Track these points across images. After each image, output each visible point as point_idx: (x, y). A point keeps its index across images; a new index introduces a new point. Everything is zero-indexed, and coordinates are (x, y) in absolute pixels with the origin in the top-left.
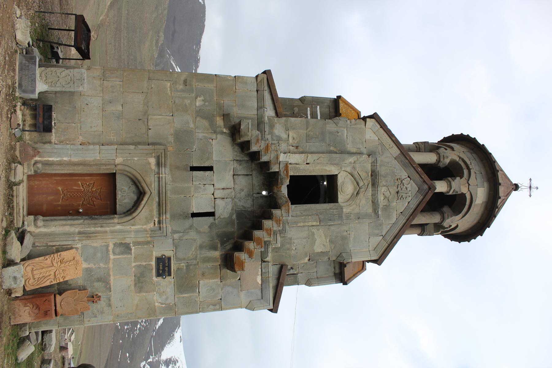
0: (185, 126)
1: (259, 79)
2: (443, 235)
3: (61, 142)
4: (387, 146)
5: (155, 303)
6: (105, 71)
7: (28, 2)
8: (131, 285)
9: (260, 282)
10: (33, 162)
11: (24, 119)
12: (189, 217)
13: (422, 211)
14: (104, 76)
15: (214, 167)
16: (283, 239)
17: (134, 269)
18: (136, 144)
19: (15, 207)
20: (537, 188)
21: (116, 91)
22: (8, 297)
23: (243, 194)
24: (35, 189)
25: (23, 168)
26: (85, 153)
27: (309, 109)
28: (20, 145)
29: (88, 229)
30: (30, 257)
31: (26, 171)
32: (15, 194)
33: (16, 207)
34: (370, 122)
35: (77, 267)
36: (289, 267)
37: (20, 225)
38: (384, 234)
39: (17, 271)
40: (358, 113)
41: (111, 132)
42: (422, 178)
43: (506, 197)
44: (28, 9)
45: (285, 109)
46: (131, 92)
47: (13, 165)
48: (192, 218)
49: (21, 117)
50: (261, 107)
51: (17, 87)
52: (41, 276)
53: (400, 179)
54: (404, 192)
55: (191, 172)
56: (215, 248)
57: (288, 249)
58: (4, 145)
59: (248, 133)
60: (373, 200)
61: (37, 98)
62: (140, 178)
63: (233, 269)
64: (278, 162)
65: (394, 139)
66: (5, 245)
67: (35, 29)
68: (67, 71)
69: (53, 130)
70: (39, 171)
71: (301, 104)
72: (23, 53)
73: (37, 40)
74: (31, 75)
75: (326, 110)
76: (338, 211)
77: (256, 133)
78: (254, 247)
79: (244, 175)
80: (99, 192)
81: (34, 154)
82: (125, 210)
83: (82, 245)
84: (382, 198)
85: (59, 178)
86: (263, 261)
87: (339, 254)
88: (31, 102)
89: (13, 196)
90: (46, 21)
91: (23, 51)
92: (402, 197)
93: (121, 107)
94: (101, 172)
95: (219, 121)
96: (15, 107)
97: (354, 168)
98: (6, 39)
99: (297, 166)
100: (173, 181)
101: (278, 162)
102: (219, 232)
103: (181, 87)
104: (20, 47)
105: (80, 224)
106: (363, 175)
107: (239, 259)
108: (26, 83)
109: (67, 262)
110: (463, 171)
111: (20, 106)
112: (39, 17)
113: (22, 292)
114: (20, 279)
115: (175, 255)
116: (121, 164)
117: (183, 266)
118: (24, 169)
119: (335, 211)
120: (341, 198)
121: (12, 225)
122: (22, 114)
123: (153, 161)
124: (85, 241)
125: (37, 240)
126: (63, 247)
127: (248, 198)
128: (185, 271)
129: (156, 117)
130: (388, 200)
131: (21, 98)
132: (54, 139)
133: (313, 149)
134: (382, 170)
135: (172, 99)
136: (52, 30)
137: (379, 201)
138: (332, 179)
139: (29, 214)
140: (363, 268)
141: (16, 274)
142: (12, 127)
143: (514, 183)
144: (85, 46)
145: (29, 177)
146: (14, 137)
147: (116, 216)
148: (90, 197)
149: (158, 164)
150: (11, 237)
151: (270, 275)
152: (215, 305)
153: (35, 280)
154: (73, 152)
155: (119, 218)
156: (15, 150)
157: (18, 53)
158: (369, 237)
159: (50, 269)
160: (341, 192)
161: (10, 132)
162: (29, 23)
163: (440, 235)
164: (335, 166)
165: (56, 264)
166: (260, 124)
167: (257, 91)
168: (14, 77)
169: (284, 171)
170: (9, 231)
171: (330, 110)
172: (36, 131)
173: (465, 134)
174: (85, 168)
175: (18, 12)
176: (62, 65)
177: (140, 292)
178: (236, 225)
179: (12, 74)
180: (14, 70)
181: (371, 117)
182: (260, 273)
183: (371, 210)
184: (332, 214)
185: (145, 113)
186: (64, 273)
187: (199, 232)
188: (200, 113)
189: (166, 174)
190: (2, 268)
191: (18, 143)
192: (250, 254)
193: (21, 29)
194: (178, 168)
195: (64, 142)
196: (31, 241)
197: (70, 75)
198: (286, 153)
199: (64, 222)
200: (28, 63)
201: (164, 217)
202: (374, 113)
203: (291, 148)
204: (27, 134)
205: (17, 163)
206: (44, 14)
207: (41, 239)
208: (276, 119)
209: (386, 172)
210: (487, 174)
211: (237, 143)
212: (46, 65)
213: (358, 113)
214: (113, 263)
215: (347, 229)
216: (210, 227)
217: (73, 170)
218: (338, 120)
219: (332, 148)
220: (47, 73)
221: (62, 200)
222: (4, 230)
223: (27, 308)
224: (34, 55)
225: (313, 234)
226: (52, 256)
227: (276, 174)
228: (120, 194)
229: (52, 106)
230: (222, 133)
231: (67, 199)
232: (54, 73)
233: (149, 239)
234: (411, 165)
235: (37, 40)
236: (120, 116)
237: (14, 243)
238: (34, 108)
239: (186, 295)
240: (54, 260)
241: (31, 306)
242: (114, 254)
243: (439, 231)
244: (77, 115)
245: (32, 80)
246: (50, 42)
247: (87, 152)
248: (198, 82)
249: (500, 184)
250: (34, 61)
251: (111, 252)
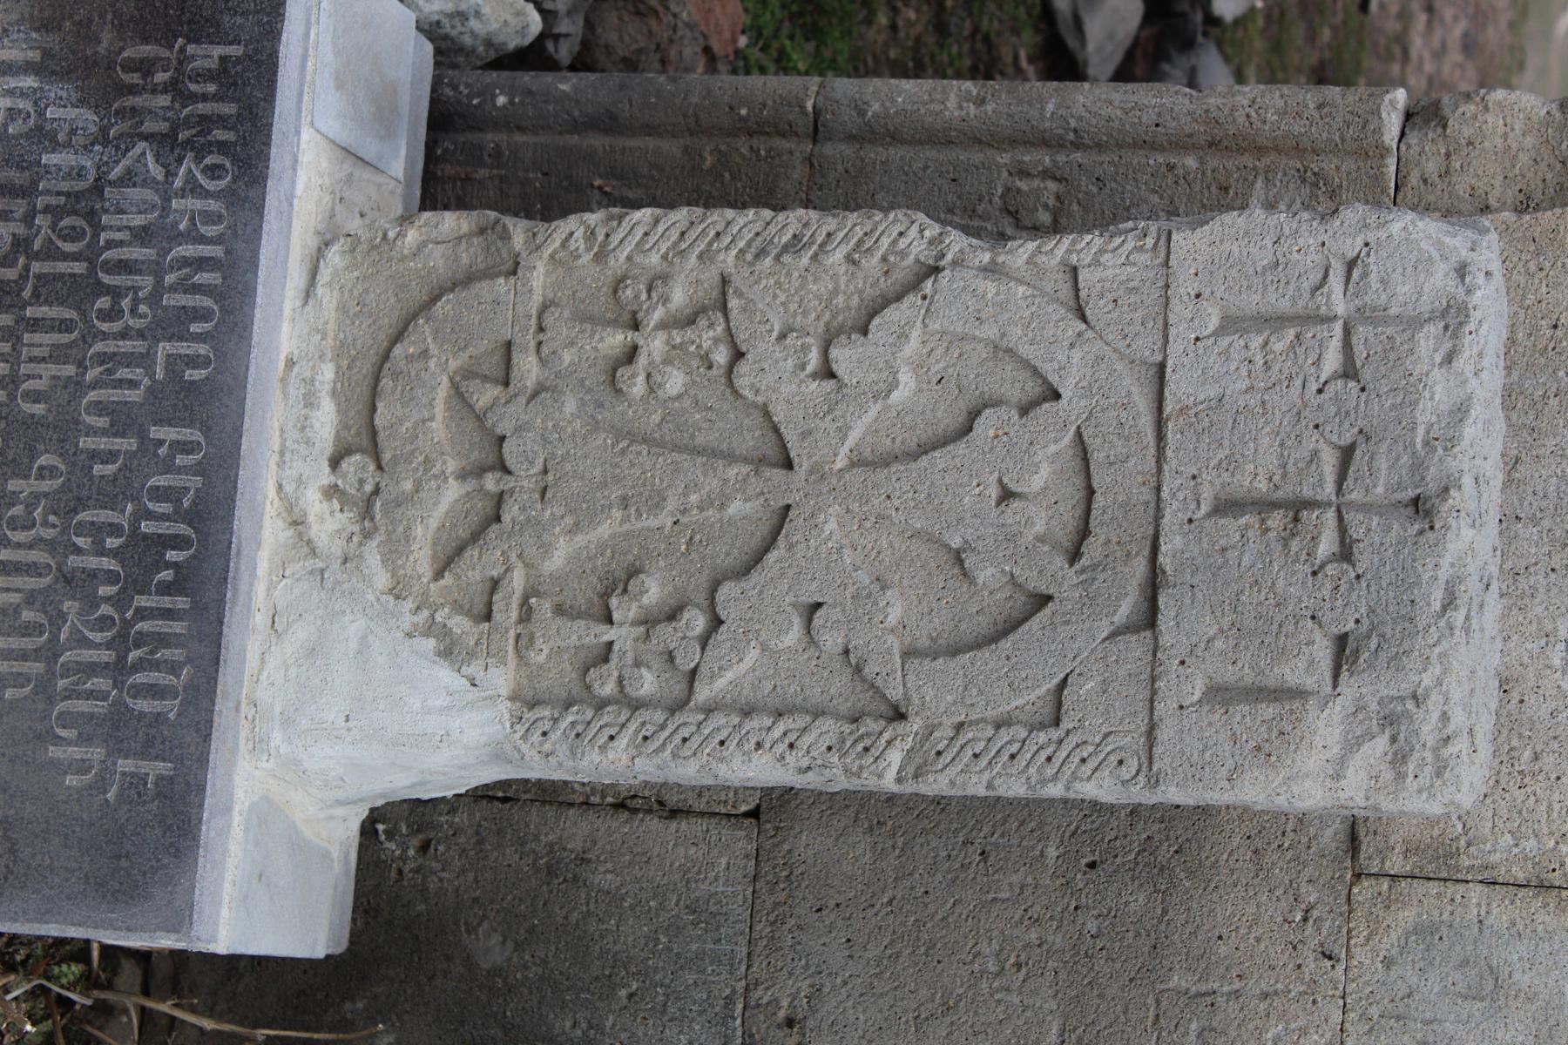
74: (121, 420)
197: (1072, 404)
200: (87, 118)
212: (609, 123)
220: (528, 368)
232: (676, 354)
250: (223, 73)
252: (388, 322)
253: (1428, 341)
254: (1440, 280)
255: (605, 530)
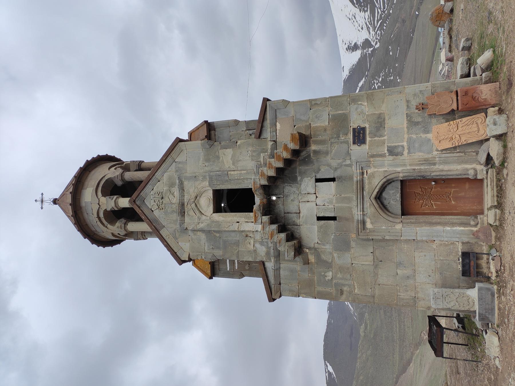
0: (341, 255)
1: (279, 294)
2: (122, 161)
3: (453, 244)
4: (171, 236)
5: (367, 105)
6: (414, 305)
7: (488, 371)
8: (388, 120)
9: (278, 123)
10: (479, 226)
11: (488, 264)
12: (337, 178)
13: (141, 182)
14: (415, 301)
15: (316, 220)
16: (258, 160)
17: (386, 133)
18: (384, 240)
19: (495, 187)
20: (36, 201)
21: (403, 287)
22: (502, 107)
23: (292, 198)
24: (476, 202)
25: (487, 221)
26: (430, 233)
27: (236, 268)
28: (491, 242)
29: (427, 167)
30: (481, 142)
31: (485, 218)
32: (495, 199)
33: (494, 186)
34: (185, 257)
35: (438, 134)
36: (253, 136)
37: (490, 171)
38: (174, 163)
39: (493, 131)
40: (195, 264)
41: (407, 250)
42: (141, 210)
43: (64, 193)
44: (488, 364)
45: (256, 268)
46: (389, 285)
47: (497, 223)
48: (335, 177)
49: (491, 266)
50: (277, 270)
51: (496, 293)
52: (470, 126)
53: (160, 209)
54: (157, 198)
55: (335, 216)
56: (315, 152)
57: (254, 151)
58: (507, 242)
59: (288, 248)
60: (183, 192)
61: (476, 283)
62: (380, 211)
63: (300, 135)
64: (262, 224)
65: (165, 243)
66: (505, 153)
67: (481, 346)
68: (449, 306)
69: (460, 254)
70: (473, 218)
71: (242, 272)
72: (491, 324)
73: (479, 336)
74: (483, 304)
75: (222, 266)
76: (213, 182)
77: (281, 249)
78: (282, 153)
79: (291, 213)
80: (416, 199)
81: (478, 233)
82: (393, 184)
83: (432, 154)
84: (175, 193)
85: (454, 211)
86: (275, 141)
87: (211, 147)
88: (482, 279)
89: (497, 196)
90: (471, 352)
91: (492, 326)
92: (159, 194)
93: (398, 272)
94: (415, 217)
95: (312, 258)
96: (497, 275)
97: (199, 219)
98: (508, 338)
99: (246, 221)
100: (350, 208)
101: (262, 224)
102: (312, 166)
103: (345, 289)
104: (494, 330)
105: (434, 171)
106: (191, 213)
107: (295, 143)
108: (487, 297)
109: (446, 139)
110: (103, 215)
111: (492, 276)
112: (477, 357)
113: (488, 112)
114: (490, 123)
115: (349, 146)
116: (397, 223)
117: (342, 137)
118: (487, 219)
119: (215, 183)
120: (210, 194)
121: (497, 170)
122: (490, 269)
123: (369, 225)
124: (430, 157)
125: (474, 157)
126: (450, 152)
127: (288, 193)
128: (341, 133)
129: (367, 263)
130: (170, 192)
131: (492, 284)
132: (459, 246)
133: (233, 234)
134: (175, 216)
135: (353, 278)
136: (464, 343)
137: (178, 191)
138: (217, 209)
139: (482, 180)
140: (191, 134)
141: (494, 127)
142: (499, 258)
143: (57, 205)
144: (433, 328)
145: (482, 213)
146: (497, 249)
147: (401, 179)
148: (424, 195)
149: (364, 223)
150: (499, 160)
151: (269, 130)
152: (316, 104)
153: (476, 123)
154: (441, 234)
155: (398, 177)
156: (496, 237)
157: (496, 324)
158: (186, 161)
159: (462, 133)
160: (210, 198)
161: (501, 253)
162: (486, 351)
163: (124, 161)
164: (215, 220)
165: (456, 137)
166: (278, 255)
167: (280, 284)
168: (500, 303)
169: (258, 216)
170: (500, 165)
171: (218, 266)
172: (477, 253)
173: (101, 248)
174: (430, 220)
175: (497, 362)
176: (454, 312)
177: (380, 114)
178: (298, 172)
179: (501, 306)
180: (499, 309)
181: (185, 261)
182: (278, 131)
183: (185, 184)
184: (218, 180)
185: (376, 266)
186: (449, 129)
187: (329, 165)
188: (328, 265)
189: (357, 214)
190: (507, 133)
191: (493, 243)
192: (286, 147)
193: (494, 346)
194: (347, 219)
195: (450, 243)
196: (479, 157)
197: (446, 302)
198: (256, 231)
199: (449, 173)
201: (358, 178)
202: (181, 265)
203: (251, 235)
204: (485, 251)
205: (494, 226)
206: (473, 360)
207: (471, 159)
208: (264, 260)
209: (172, 215)
210: (82, 213)
211: (297, 240)
213: (194, 264)
214: (404, 138)
215: (205, 168)
216: (319, 170)
217: (441, 218)
218: (212, 259)
219: (218, 235)
220: (467, 305)
221: (451, 192)
222: (506, 167)
223: (484, 98)
224: (481, 322)
225: (233, 164)
226: (460, 144)
227: (264, 214)
228: (397, 197)
229: (462, 276)
230: (309, 248)
231: (446, 193)
233: (372, 159)
234: (150, 221)
235: (479, 336)
236: (399, 264)
237: (496, 155)
238: (479, 274)
239: (340, 112)
240: (458, 140)
241: (480, 99)
242: (403, 147)
243: (125, 164)
244: (439, 266)
245: (482, 299)
246: (466, 333)
247: (429, 234)
248: (331, 293)
249: (70, 205)
251: (406, 149)
252: (473, 307)
253: (433, 304)
254: (433, 305)
255: (463, 299)
